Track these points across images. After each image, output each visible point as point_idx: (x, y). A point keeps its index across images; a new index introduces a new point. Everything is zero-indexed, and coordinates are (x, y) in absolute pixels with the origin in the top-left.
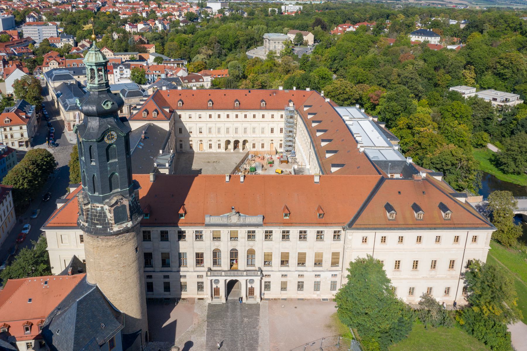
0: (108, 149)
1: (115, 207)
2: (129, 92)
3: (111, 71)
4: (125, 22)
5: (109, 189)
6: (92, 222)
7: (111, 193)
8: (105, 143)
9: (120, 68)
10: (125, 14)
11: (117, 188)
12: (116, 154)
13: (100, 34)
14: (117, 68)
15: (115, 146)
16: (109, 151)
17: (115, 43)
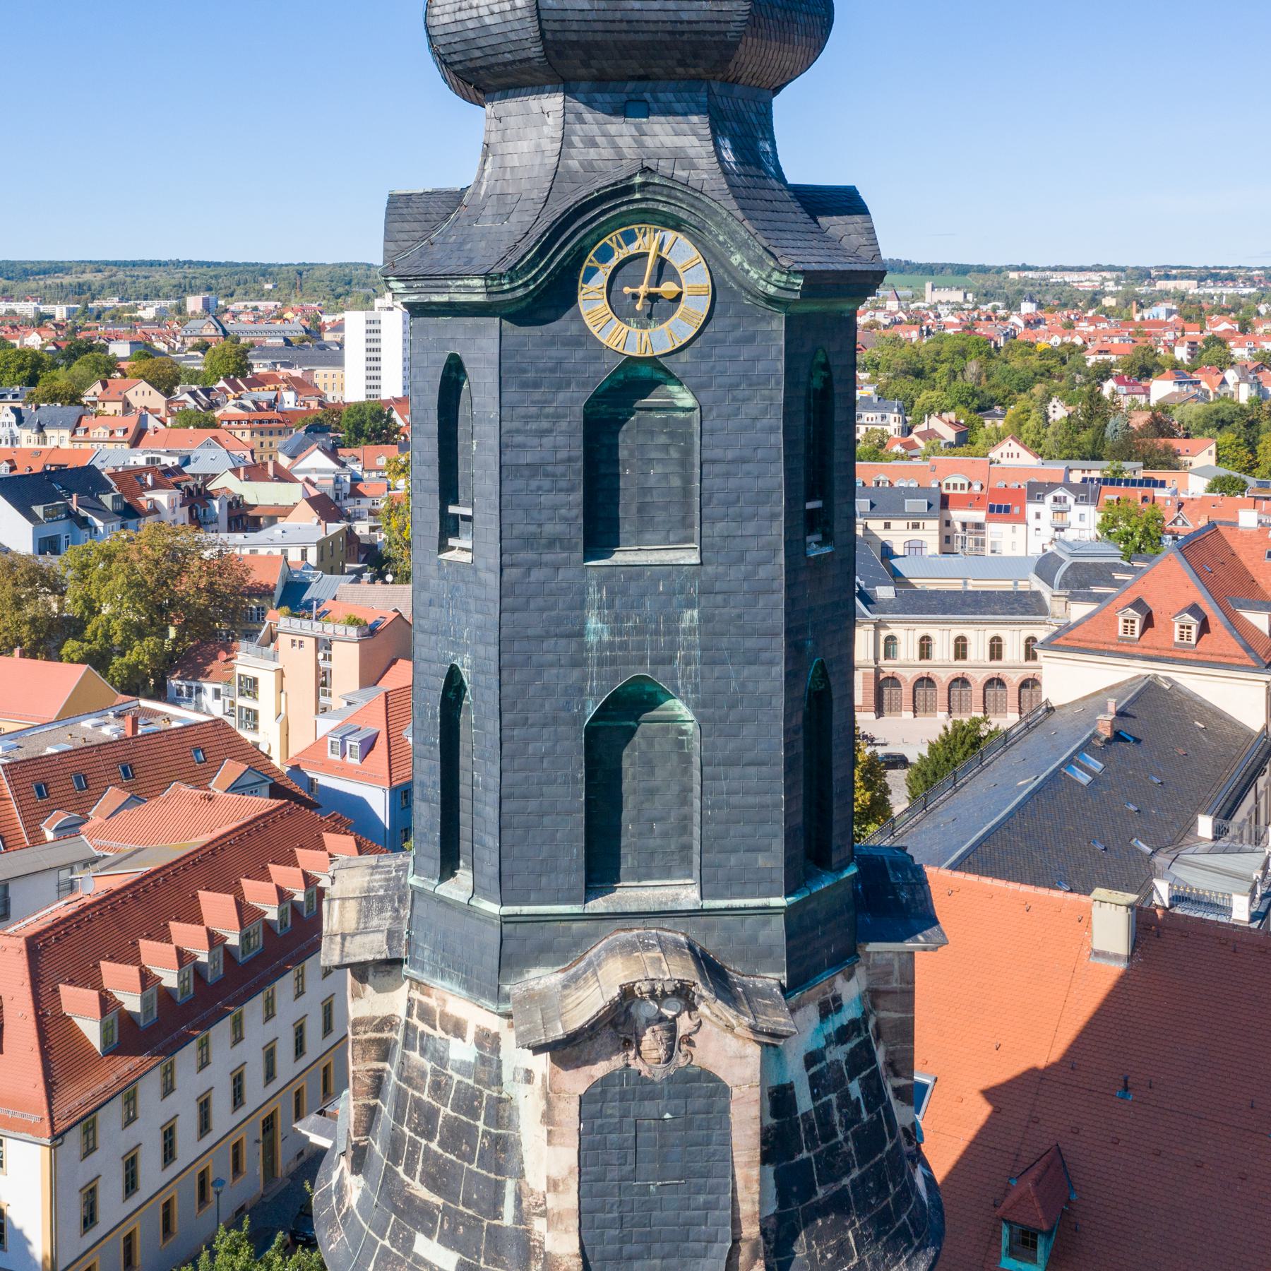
0: (615, 424)
1: (600, 1069)
2: (1074, 567)
3: (1016, 510)
4: (1104, 372)
5: (579, 849)
6: (390, 1175)
7: (599, 905)
8: (584, 338)
9: (1055, 499)
10: (1106, 352)
11: (667, 873)
12: (686, 492)
13: (1001, 404)
14: (1040, 499)
15: (685, 398)
16: (627, 442)
17: (1050, 430)
